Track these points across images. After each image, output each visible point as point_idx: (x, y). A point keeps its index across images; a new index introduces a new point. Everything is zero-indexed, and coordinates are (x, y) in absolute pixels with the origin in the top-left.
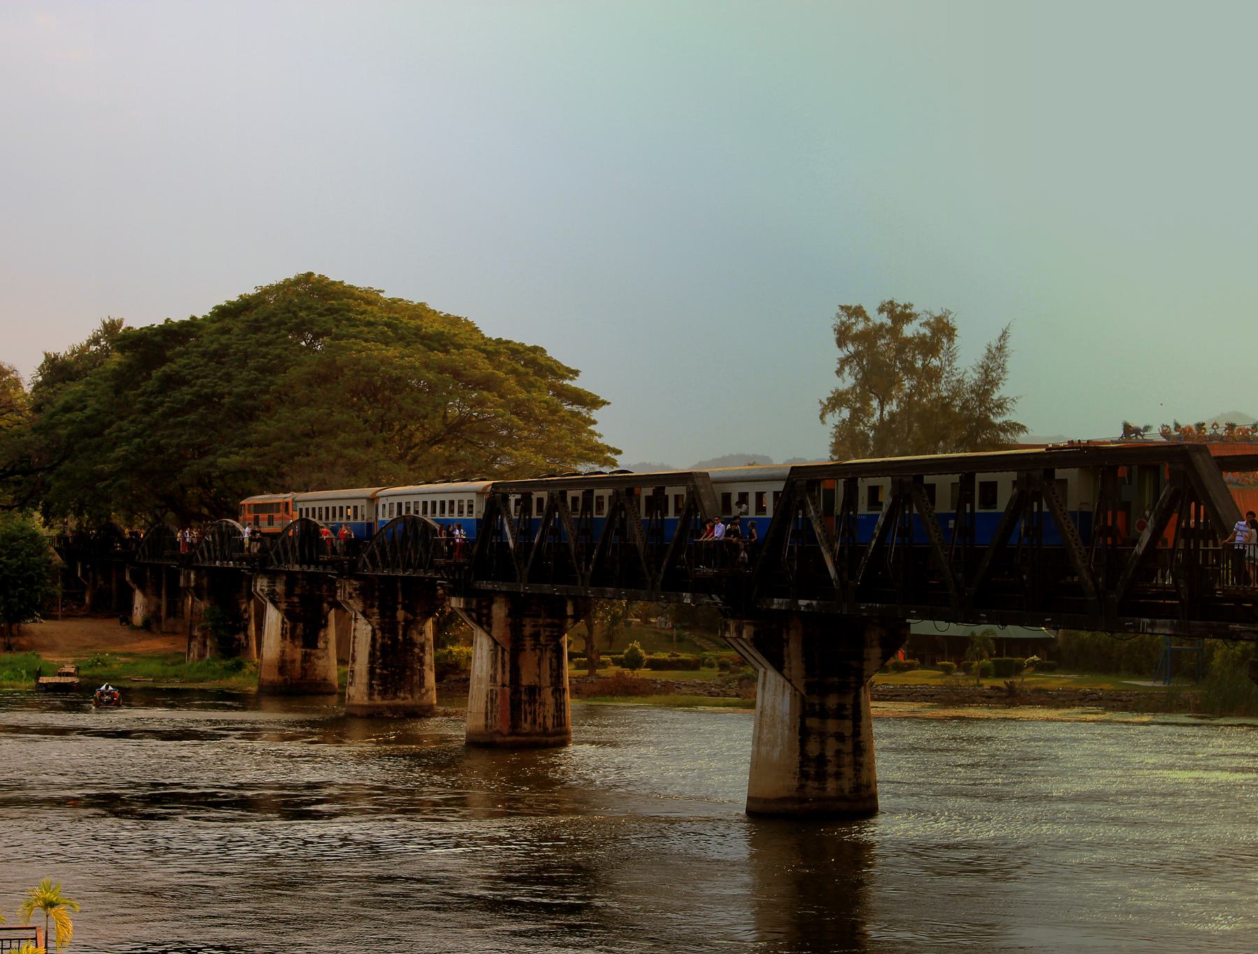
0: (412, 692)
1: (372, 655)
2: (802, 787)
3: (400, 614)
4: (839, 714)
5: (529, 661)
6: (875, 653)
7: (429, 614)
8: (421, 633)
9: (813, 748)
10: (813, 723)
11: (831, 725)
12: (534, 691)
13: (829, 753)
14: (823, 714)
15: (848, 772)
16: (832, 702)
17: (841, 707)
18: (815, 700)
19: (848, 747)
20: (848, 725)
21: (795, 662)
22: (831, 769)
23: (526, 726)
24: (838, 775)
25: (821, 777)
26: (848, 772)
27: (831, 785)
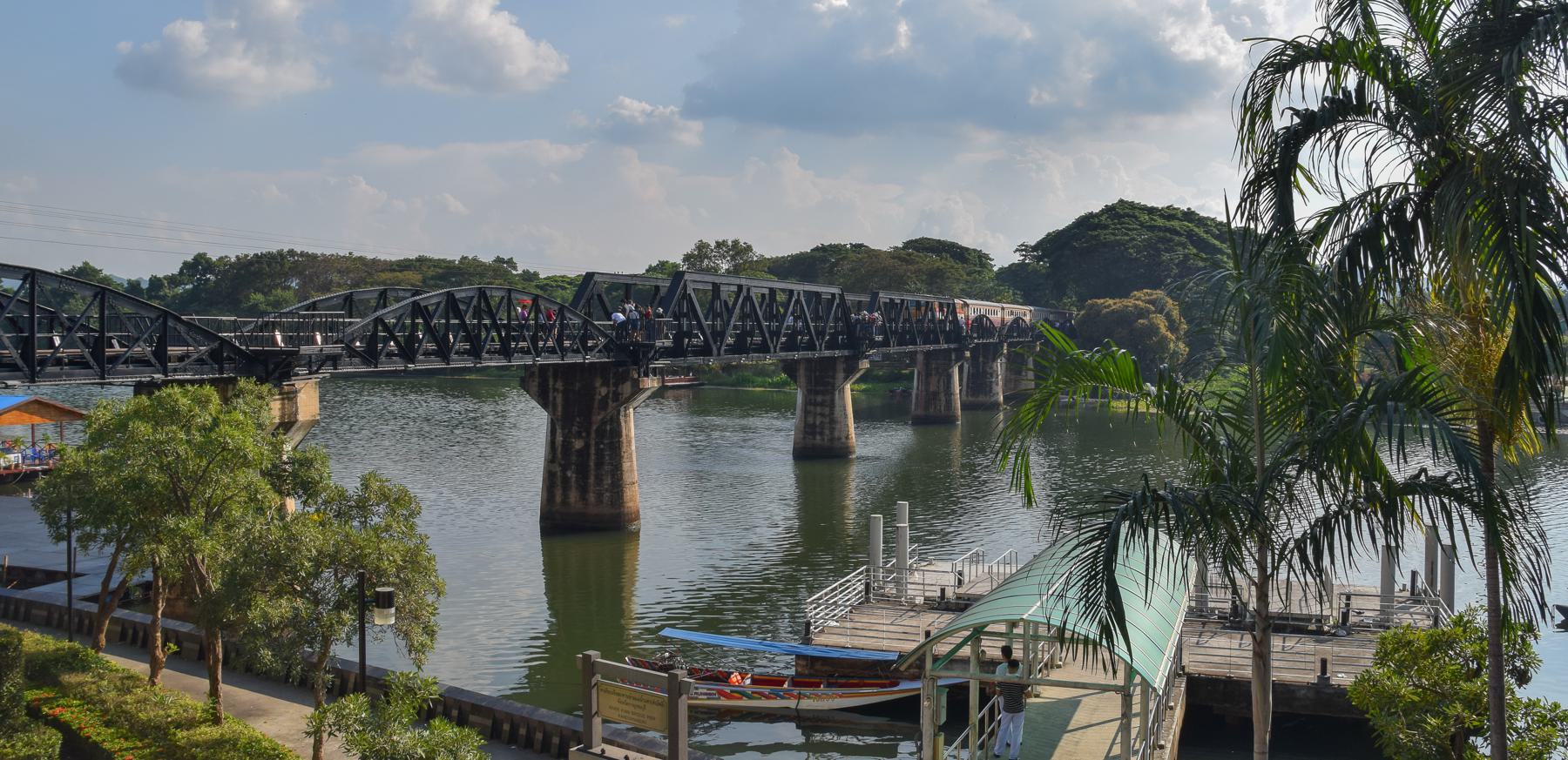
0: (986, 395)
1: (968, 378)
2: (804, 438)
3: (981, 359)
4: (822, 404)
5: (934, 380)
6: (841, 375)
7: (994, 360)
8: (991, 368)
9: (810, 420)
10: (811, 408)
11: (819, 410)
12: (936, 394)
13: (818, 423)
14: (815, 404)
15: (827, 432)
16: (819, 398)
17: (824, 401)
18: (812, 397)
19: (827, 420)
20: (827, 411)
21: (802, 379)
22: (818, 430)
23: (931, 410)
24: (821, 434)
25: (813, 434)
26: (827, 432)
27: (818, 437)
